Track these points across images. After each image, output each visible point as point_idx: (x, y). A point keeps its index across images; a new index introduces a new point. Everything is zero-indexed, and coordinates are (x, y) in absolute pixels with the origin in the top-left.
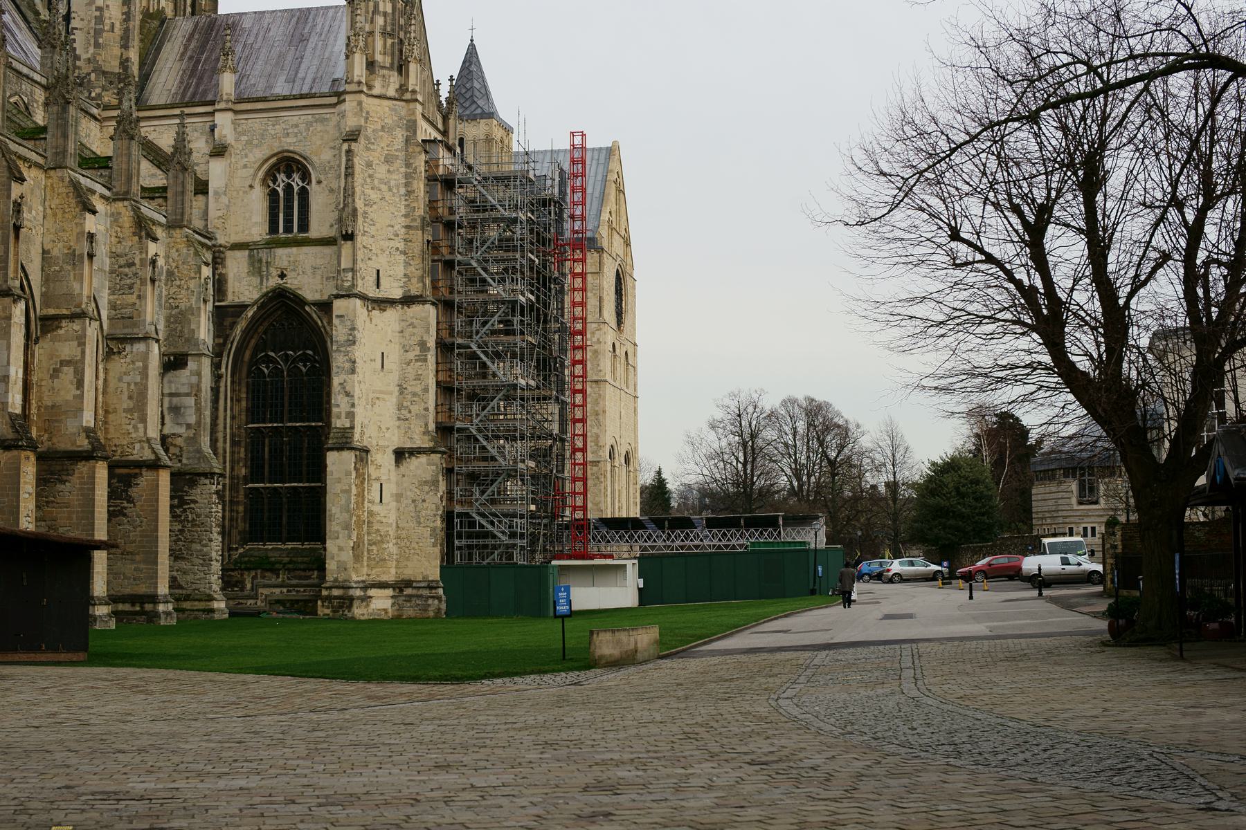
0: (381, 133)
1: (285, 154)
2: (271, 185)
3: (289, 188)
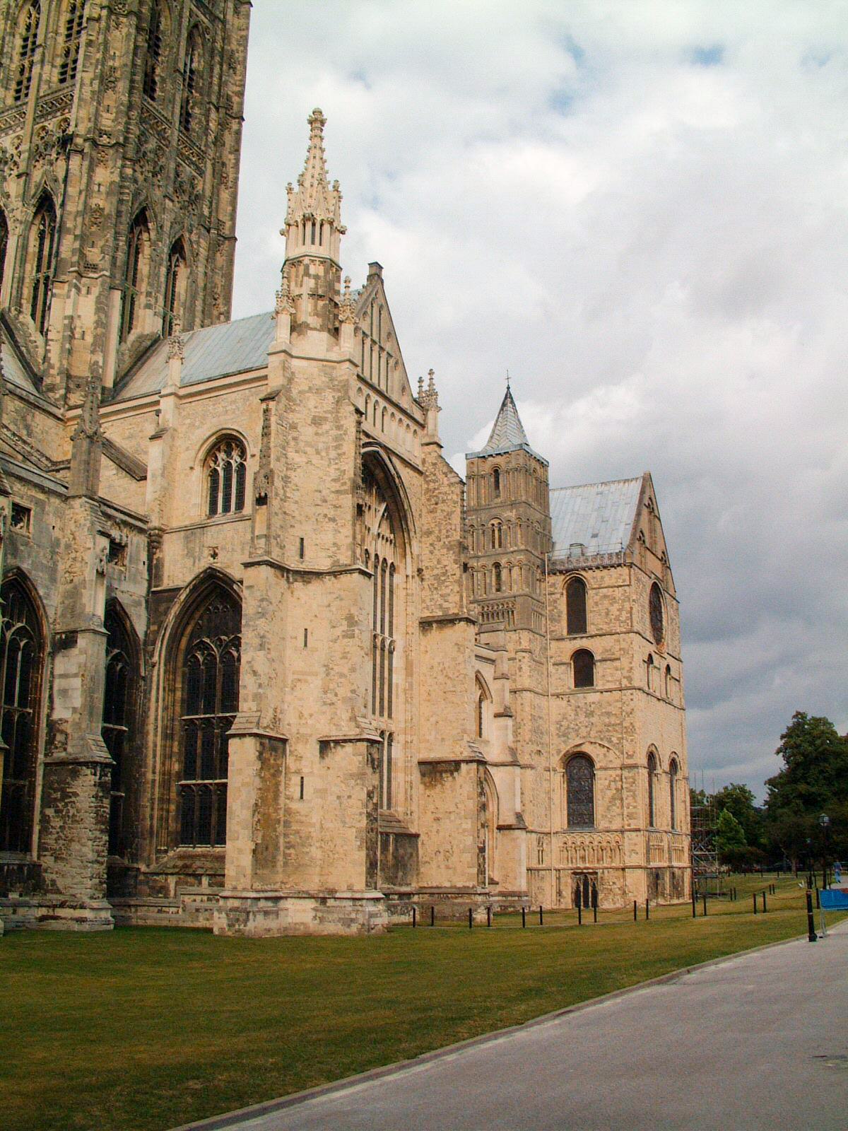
0: (307, 395)
1: (224, 432)
2: (212, 465)
3: (228, 466)
